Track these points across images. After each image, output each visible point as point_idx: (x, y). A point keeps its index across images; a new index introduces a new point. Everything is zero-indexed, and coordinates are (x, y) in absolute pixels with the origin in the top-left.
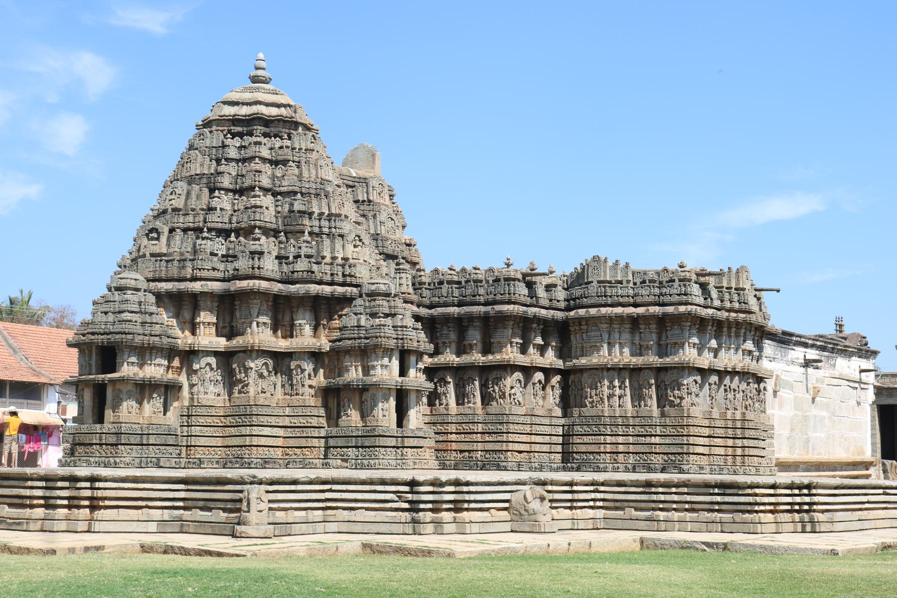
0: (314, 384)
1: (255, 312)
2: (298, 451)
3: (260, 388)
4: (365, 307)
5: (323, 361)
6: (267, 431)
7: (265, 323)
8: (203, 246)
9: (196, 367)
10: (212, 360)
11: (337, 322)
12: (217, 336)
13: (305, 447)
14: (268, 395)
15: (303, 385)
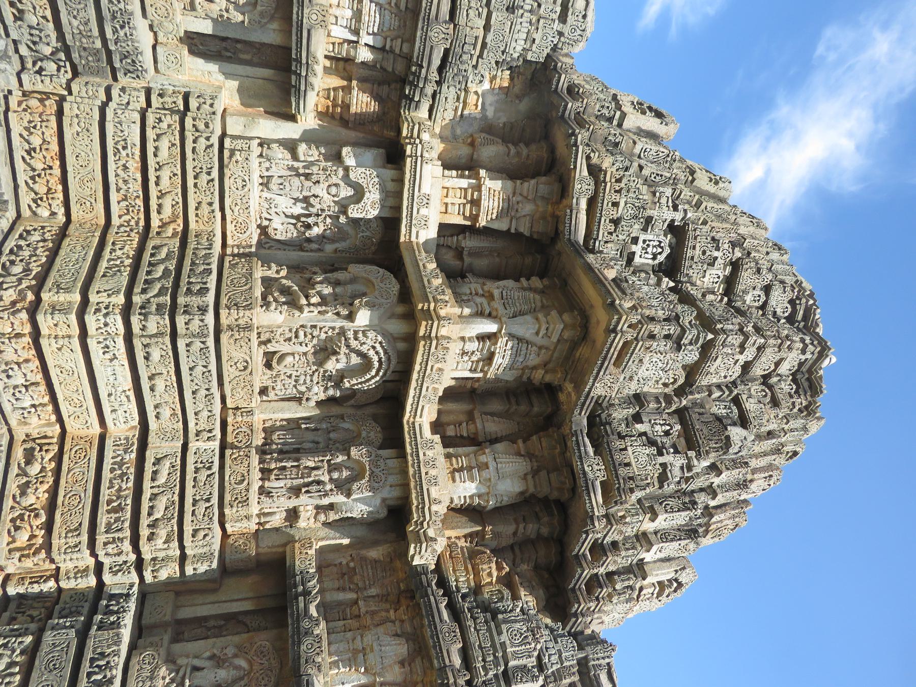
0: (302, 524)
1: (526, 328)
2: (38, 497)
3: (285, 348)
4: (558, 676)
5: (375, 543)
6: (114, 375)
7: (490, 358)
8: (663, 200)
9: (349, 156)
10: (370, 208)
11: (495, 574)
12: (443, 227)
13: (49, 527)
14: (261, 378)
15: (296, 491)
